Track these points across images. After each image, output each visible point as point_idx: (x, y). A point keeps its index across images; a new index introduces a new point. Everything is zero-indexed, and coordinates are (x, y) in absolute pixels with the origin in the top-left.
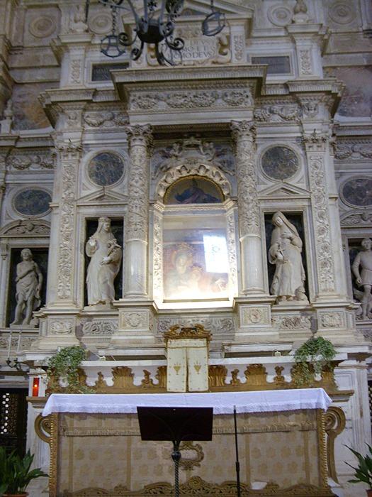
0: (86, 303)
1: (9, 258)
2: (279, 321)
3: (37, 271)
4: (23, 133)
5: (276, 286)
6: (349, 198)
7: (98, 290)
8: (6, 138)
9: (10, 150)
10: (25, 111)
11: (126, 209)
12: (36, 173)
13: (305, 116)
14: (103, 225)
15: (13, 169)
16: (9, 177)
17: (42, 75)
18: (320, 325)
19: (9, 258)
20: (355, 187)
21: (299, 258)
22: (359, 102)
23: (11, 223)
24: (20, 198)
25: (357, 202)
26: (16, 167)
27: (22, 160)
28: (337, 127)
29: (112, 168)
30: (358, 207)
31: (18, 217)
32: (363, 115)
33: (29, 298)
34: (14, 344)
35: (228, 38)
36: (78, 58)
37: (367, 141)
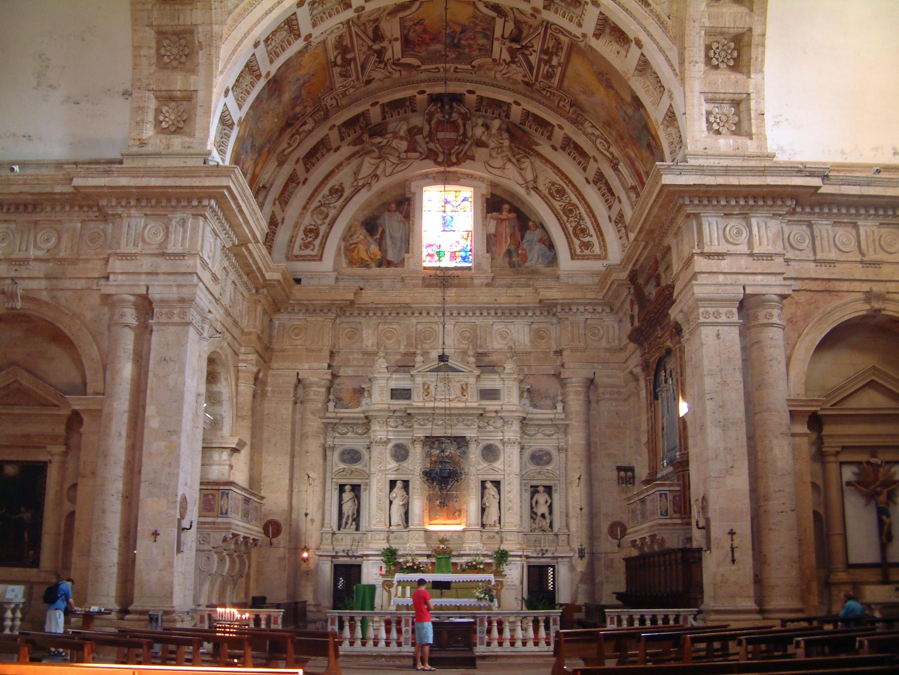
0: (390, 525)
2: (485, 536)
5: (485, 519)
7: (397, 518)
8: (334, 418)
10: (342, 395)
11: (410, 476)
12: (352, 438)
13: (506, 428)
15: (337, 435)
18: (504, 539)
21: (497, 505)
24: (343, 453)
25: (538, 464)
29: (403, 452)
31: (342, 466)
33: (350, 513)
35: (467, 384)
36: (383, 385)
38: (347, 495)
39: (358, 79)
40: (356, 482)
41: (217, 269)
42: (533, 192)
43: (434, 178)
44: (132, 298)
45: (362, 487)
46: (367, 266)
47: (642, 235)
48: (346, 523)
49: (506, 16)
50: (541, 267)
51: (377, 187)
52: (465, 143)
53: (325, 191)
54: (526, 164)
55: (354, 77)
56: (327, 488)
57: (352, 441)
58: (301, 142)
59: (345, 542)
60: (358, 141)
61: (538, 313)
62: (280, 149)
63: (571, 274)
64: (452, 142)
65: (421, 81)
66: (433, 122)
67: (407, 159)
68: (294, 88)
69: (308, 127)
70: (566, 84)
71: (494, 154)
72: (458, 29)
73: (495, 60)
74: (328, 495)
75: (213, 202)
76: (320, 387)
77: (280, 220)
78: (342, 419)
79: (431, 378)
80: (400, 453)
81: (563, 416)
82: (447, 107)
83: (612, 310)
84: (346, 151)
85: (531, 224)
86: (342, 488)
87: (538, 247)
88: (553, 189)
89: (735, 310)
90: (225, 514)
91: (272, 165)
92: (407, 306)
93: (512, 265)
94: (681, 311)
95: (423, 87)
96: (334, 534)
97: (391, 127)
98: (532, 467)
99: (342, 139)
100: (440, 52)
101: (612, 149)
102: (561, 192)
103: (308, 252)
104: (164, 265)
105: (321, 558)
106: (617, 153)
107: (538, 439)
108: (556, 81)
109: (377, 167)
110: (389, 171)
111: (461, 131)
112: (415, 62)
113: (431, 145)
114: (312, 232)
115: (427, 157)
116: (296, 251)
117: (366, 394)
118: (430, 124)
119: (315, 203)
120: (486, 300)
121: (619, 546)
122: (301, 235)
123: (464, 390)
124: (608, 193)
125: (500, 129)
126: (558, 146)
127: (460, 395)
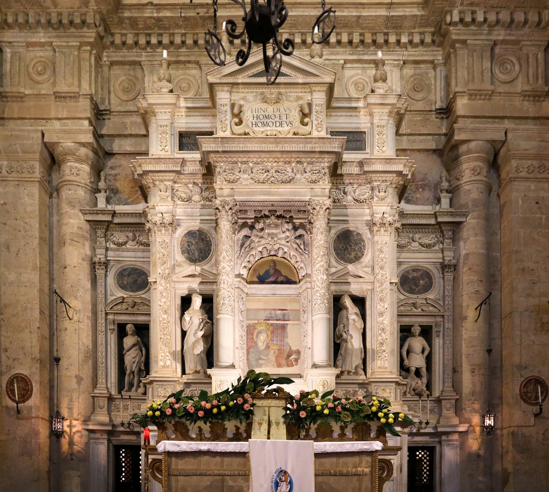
1: (116, 332)
3: (141, 344)
4: (119, 208)
6: (405, 287)
9: (108, 226)
12: (134, 251)
15: (112, 246)
16: (110, 253)
17: (131, 145)
19: (116, 332)
20: (411, 277)
22: (423, 190)
23: (115, 299)
24: (121, 275)
26: (115, 244)
27: (119, 237)
28: (402, 214)
30: (411, 296)
31: (120, 293)
32: (426, 203)
34: (126, 408)
37: (426, 230)
56: (99, 328)
74: (101, 338)
96: (110, 399)
105: (92, 435)
107: (413, 252)
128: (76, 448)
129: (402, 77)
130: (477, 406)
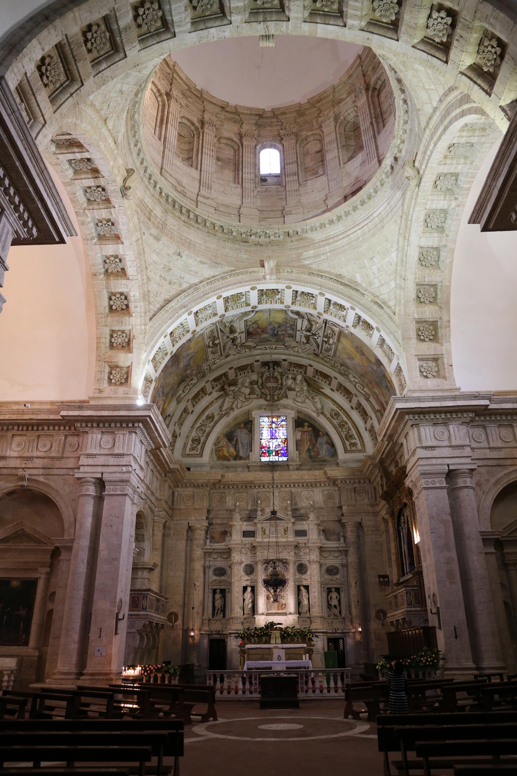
10: (214, 535)
14: (249, 589)
25: (331, 574)
31: (215, 578)
33: (219, 607)
38: (218, 596)
39: (221, 354)
40: (223, 587)
41: (143, 464)
42: (321, 415)
43: (265, 409)
44: (93, 480)
45: (227, 591)
46: (228, 460)
47: (386, 438)
48: (217, 613)
49: (303, 318)
50: (327, 458)
51: (233, 415)
52: (282, 389)
53: (204, 417)
54: (317, 399)
55: (219, 354)
57: (220, 563)
58: (190, 390)
59: (216, 626)
60: (222, 389)
61: (327, 485)
62: (178, 394)
63: (345, 462)
64: (275, 389)
65: (257, 355)
66: (264, 378)
67: (250, 398)
68: (186, 360)
69: (194, 382)
70: (338, 354)
71: (298, 394)
72: (277, 326)
73: (297, 342)
75: (141, 425)
76: (202, 530)
77: (178, 434)
78: (214, 549)
79: (266, 525)
80: (250, 570)
81: (344, 545)
82: (272, 369)
83: (370, 482)
84: (215, 394)
85: (321, 433)
86: (214, 591)
87: (325, 446)
88: (333, 413)
89: (444, 479)
90: (145, 609)
91: (174, 403)
92: (252, 482)
93: (311, 457)
94: (412, 481)
95: (258, 358)
96: (209, 620)
97: (240, 381)
98: (327, 577)
99: (213, 388)
100: (267, 338)
101: (365, 389)
102: (337, 415)
103: (194, 452)
104: (112, 461)
106: (368, 391)
108: (332, 353)
109: (233, 403)
110: (239, 406)
111: (280, 382)
112: (253, 344)
113: (263, 391)
114: (196, 441)
115: (261, 397)
116: (187, 452)
117: (228, 535)
118: (262, 379)
119: (198, 424)
120: (297, 478)
121: (383, 625)
122: (190, 442)
123: (286, 531)
124: (364, 414)
125: (301, 381)
126: (334, 389)
127: (283, 534)
128: (196, 641)
129: (323, 494)
130: (358, 621)
